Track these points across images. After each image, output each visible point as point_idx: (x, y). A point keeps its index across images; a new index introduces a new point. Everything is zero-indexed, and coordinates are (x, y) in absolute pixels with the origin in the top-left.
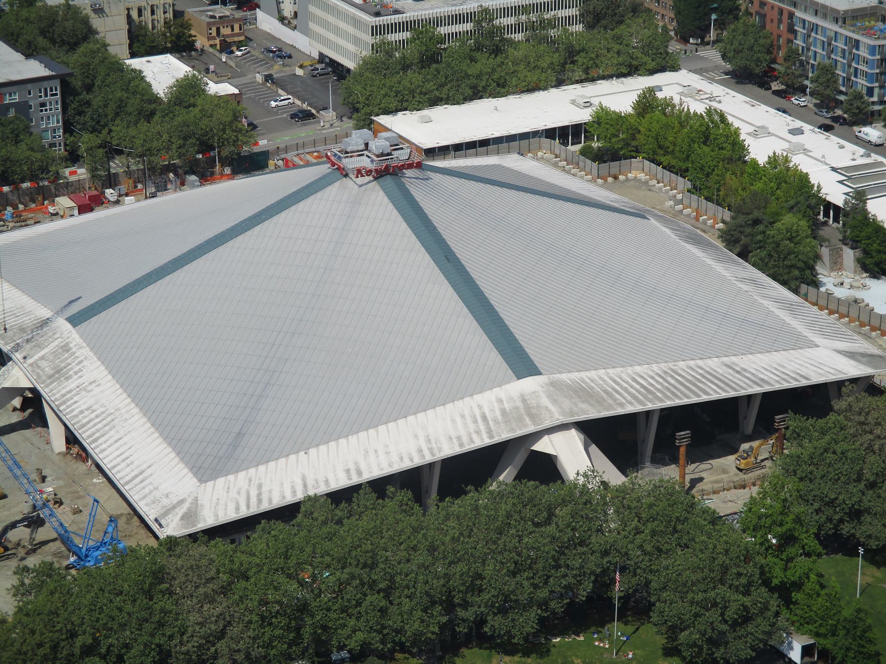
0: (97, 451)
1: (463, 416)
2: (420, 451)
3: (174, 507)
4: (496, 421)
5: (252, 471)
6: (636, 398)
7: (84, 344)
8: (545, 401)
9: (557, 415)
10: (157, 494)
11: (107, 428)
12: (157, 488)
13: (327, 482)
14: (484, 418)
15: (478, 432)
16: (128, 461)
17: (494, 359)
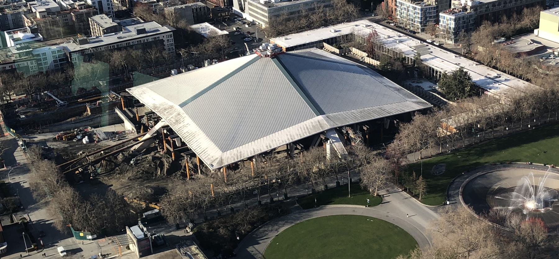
0: (190, 145)
1: (301, 128)
2: (288, 139)
3: (215, 160)
4: (311, 129)
5: (238, 148)
6: (352, 119)
7: (185, 113)
8: (325, 122)
9: (329, 126)
10: (209, 157)
11: (193, 138)
12: (209, 155)
13: (261, 150)
14: (307, 128)
15: (306, 133)
16: (200, 147)
17: (308, 109)
